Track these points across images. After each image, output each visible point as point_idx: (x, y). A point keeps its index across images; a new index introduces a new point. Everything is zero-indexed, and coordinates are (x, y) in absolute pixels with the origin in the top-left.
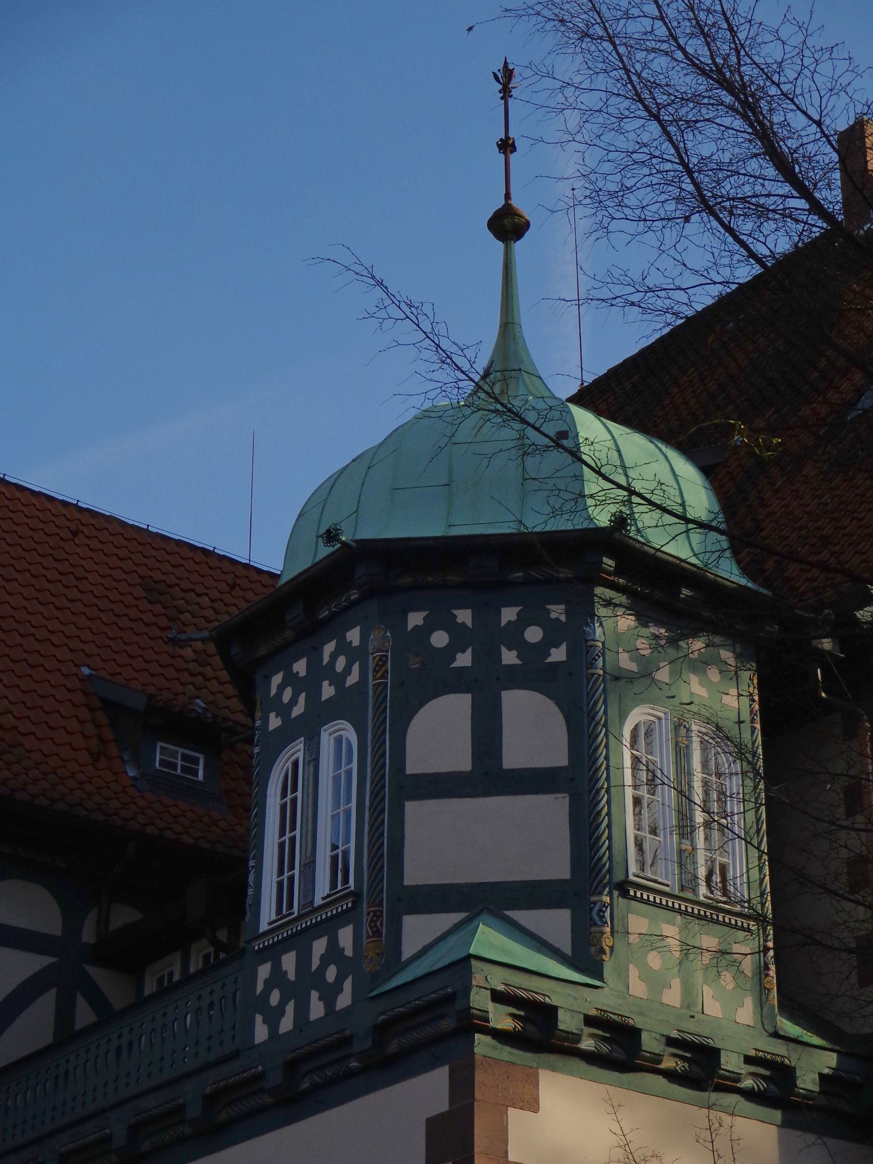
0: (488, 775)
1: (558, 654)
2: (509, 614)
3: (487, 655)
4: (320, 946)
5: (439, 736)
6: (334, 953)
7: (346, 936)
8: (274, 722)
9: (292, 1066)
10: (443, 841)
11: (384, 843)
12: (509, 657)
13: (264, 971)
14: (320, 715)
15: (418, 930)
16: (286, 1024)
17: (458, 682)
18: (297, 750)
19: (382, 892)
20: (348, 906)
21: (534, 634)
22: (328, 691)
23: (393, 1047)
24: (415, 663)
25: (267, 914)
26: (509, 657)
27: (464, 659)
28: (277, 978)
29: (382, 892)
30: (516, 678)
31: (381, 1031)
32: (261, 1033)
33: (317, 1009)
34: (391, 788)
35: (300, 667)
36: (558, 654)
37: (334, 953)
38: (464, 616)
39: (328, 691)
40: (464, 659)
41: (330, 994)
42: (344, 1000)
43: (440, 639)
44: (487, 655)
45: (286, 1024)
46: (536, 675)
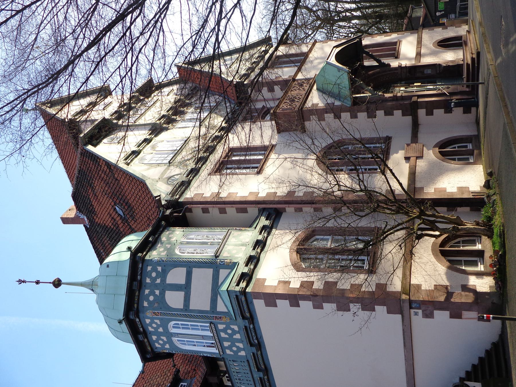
0: (186, 288)
1: (159, 269)
2: (148, 280)
3: (157, 286)
4: (223, 335)
5: (174, 299)
6: (224, 331)
7: (221, 327)
9: (252, 345)
10: (200, 300)
11: (200, 315)
12: (158, 281)
13: (228, 352)
15: (221, 307)
16: (241, 345)
17: (163, 294)
18: (175, 339)
19: (211, 316)
20: (213, 327)
21: (154, 275)
22: (161, 330)
23: (248, 315)
24: (156, 305)
25: (214, 350)
26: (158, 281)
27: (157, 292)
28: (230, 348)
29: (211, 316)
30: (164, 280)
31: (244, 318)
32: (243, 353)
33: (238, 336)
34: (186, 312)
35: (154, 338)
37: (224, 331)
38: (147, 292)
39: (161, 330)
40: (157, 292)
41: (234, 332)
42: (236, 328)
43: (151, 298)
44: (157, 286)
45: (241, 345)
46: (164, 274)
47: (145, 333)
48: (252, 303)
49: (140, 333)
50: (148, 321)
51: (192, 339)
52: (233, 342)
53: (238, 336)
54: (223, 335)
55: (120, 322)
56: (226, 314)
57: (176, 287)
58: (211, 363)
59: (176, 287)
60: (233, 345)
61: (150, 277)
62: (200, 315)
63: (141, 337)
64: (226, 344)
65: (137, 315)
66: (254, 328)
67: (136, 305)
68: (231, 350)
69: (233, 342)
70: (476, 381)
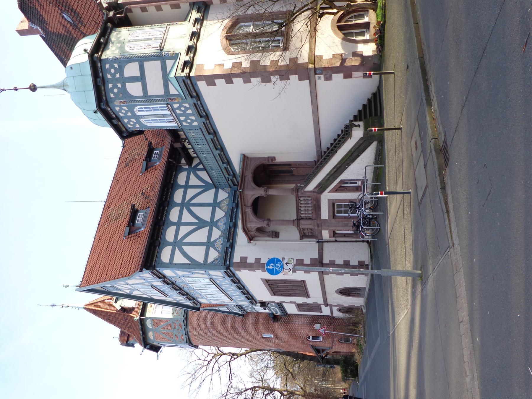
0: (142, 78)
1: (116, 65)
2: (109, 76)
3: (118, 80)
5: (134, 89)
6: (179, 108)
7: (176, 106)
8: (137, 126)
9: (201, 117)
10: (155, 87)
11: (157, 99)
12: (118, 76)
13: (184, 124)
14: (134, 116)
15: (173, 91)
16: (193, 118)
17: (124, 86)
18: (142, 120)
19: (166, 99)
20: (169, 106)
21: (113, 71)
22: (129, 114)
23: (195, 94)
24: (121, 95)
25: (174, 124)
26: (118, 76)
27: (119, 85)
28: (185, 121)
29: (166, 99)
30: (122, 74)
31: (192, 97)
32: (196, 123)
33: (190, 111)
34: (146, 98)
35: (126, 121)
36: (116, 65)
37: (179, 108)
38: (110, 86)
39: (129, 114)
40: (119, 85)
42: (187, 105)
43: (116, 90)
44: (118, 80)
45: (193, 118)
46: (121, 70)
47: (117, 118)
48: (196, 84)
49: (113, 119)
50: (117, 109)
51: (156, 118)
52: (187, 116)
53: (190, 111)
54: (178, 112)
55: (95, 112)
56: (178, 95)
57: (133, 79)
58: (174, 133)
59: (133, 79)
60: (187, 118)
61: (110, 73)
62: (157, 99)
63: (115, 122)
64: (182, 118)
65: (107, 104)
66: (201, 103)
67: (104, 98)
68: (187, 122)
69: (187, 116)
70: (360, 120)
